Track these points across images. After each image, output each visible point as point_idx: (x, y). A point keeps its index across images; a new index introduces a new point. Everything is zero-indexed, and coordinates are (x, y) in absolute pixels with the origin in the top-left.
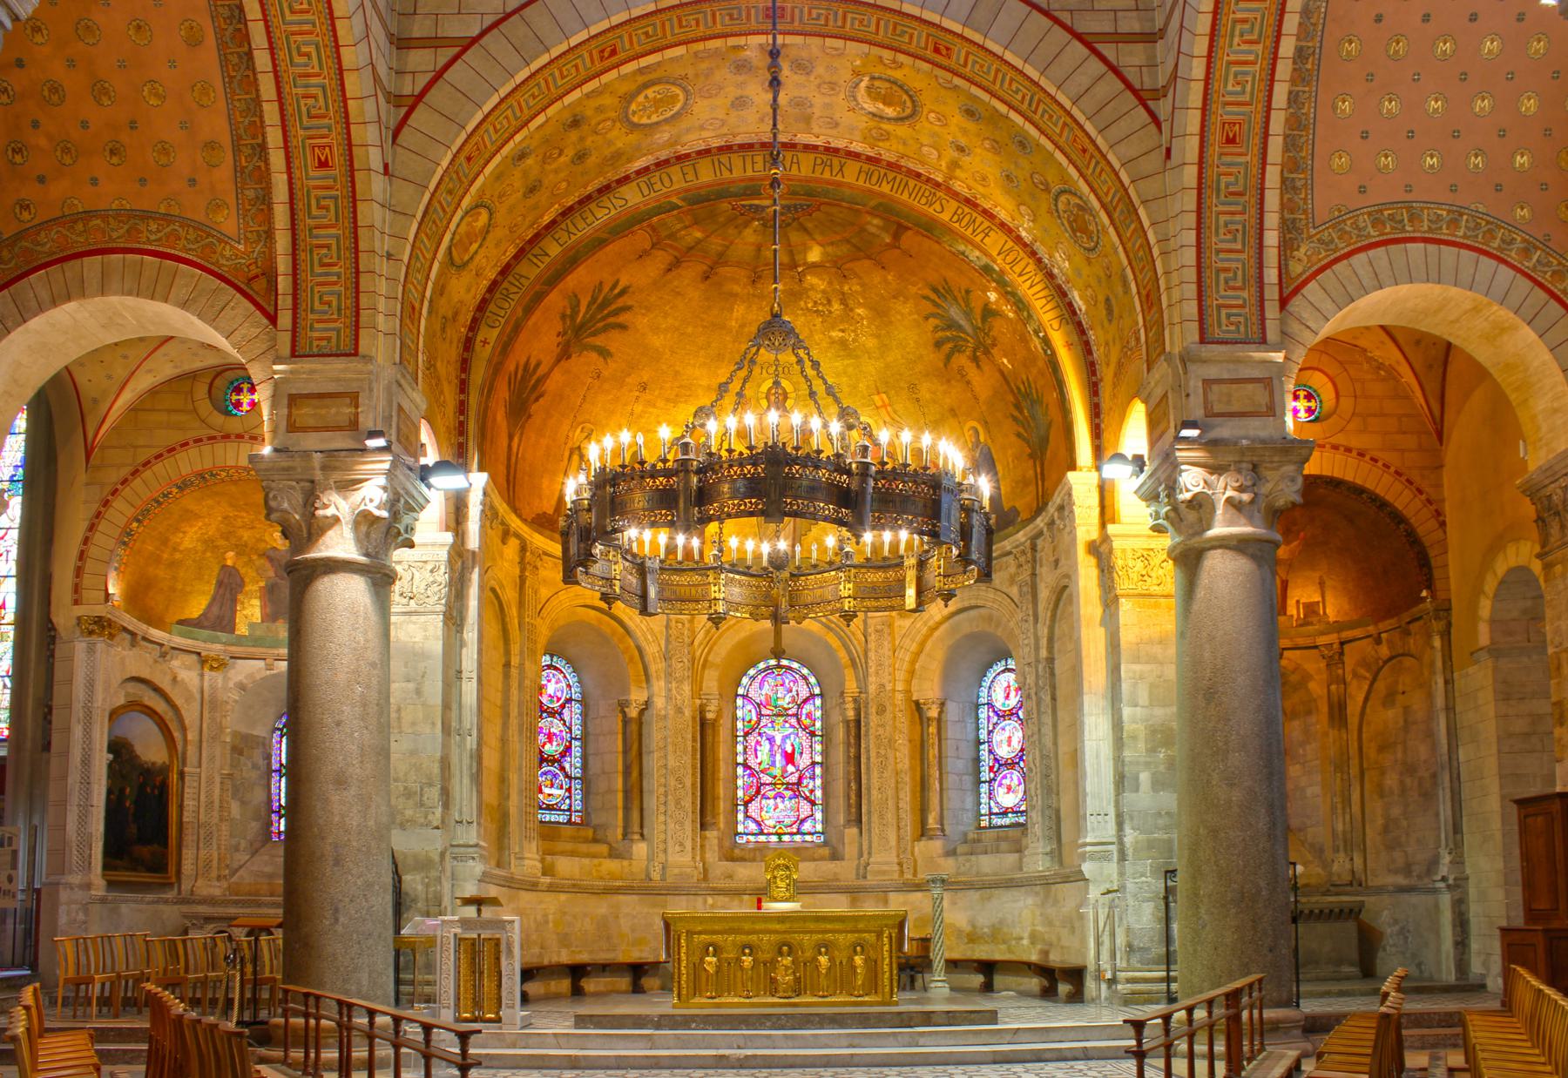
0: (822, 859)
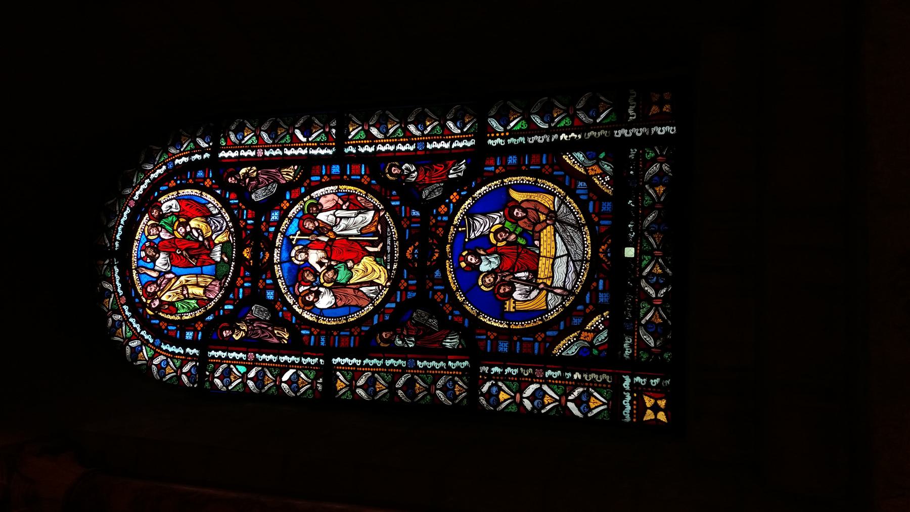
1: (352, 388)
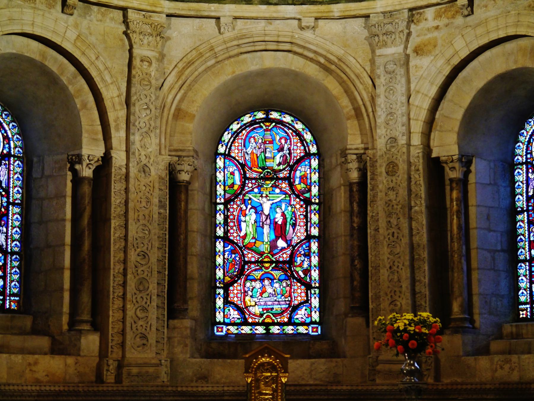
0: (319, 355)
1: (519, 221)
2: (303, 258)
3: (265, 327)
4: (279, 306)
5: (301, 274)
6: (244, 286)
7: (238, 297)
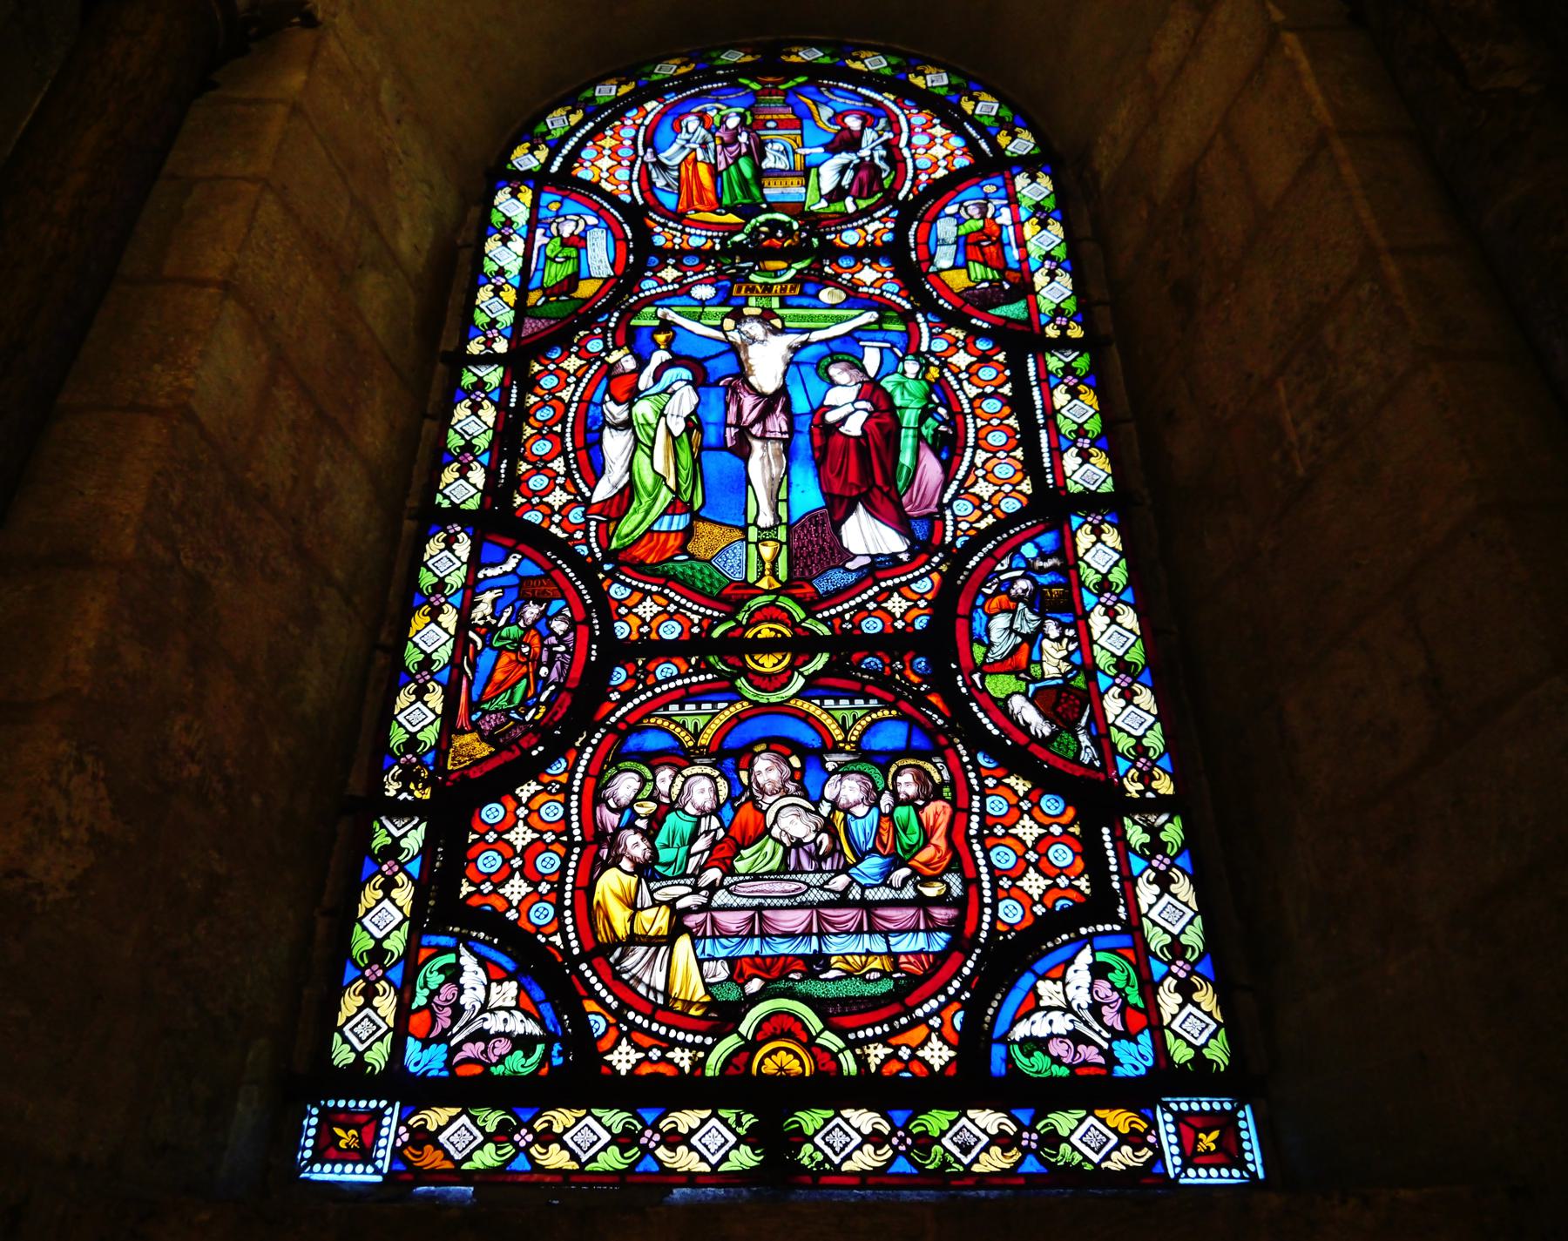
2: (1027, 621)
3: (748, 1119)
4: (878, 945)
5: (1029, 714)
6: (596, 795)
7: (533, 879)
